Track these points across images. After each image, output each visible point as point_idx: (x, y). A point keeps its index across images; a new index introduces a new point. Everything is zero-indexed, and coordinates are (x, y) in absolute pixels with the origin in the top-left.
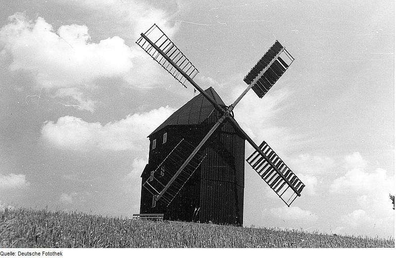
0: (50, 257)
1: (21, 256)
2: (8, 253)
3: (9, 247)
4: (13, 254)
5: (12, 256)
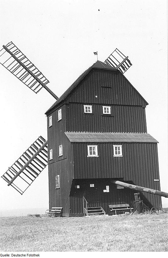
0: (32, 257)
1: (14, 257)
2: (5, 255)
3: (6, 251)
4: (8, 255)
5: (8, 257)
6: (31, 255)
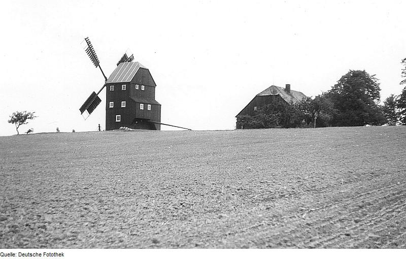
2: (9, 254)
4: (13, 255)
6: (49, 255)
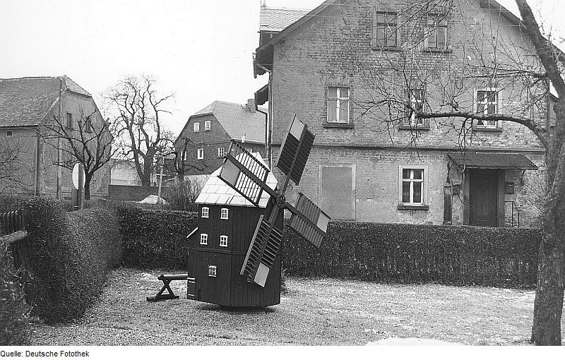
2: (12, 353)
4: (18, 354)
5: (17, 358)
6: (69, 354)
